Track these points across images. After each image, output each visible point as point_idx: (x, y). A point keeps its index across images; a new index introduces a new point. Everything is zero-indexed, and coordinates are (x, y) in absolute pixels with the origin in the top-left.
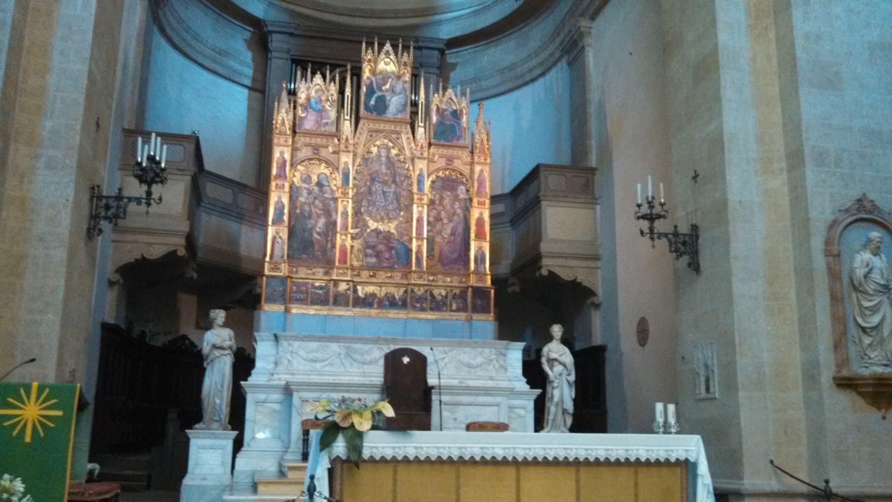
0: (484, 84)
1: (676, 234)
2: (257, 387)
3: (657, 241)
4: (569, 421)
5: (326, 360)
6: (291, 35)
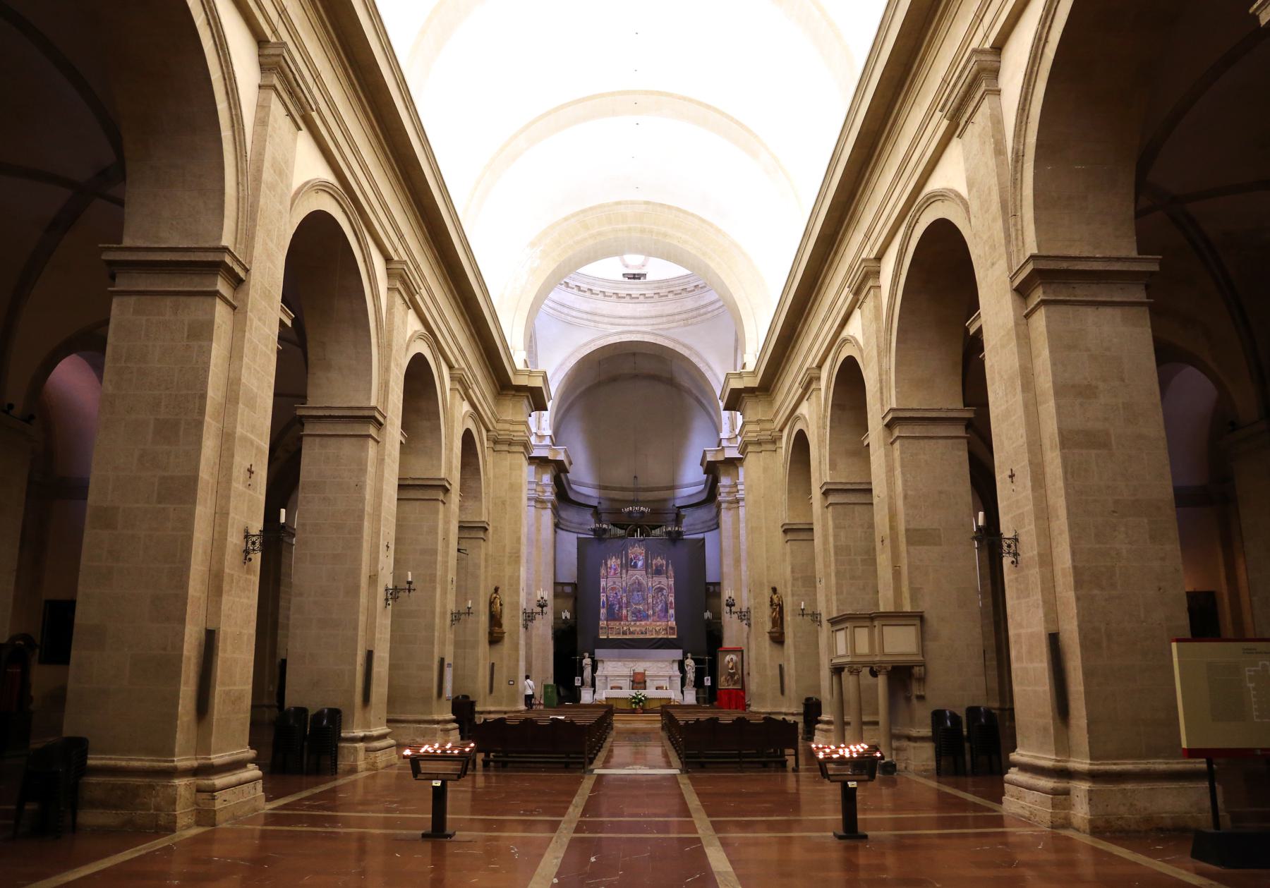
0: (697, 527)
1: (741, 612)
2: (598, 676)
3: (733, 615)
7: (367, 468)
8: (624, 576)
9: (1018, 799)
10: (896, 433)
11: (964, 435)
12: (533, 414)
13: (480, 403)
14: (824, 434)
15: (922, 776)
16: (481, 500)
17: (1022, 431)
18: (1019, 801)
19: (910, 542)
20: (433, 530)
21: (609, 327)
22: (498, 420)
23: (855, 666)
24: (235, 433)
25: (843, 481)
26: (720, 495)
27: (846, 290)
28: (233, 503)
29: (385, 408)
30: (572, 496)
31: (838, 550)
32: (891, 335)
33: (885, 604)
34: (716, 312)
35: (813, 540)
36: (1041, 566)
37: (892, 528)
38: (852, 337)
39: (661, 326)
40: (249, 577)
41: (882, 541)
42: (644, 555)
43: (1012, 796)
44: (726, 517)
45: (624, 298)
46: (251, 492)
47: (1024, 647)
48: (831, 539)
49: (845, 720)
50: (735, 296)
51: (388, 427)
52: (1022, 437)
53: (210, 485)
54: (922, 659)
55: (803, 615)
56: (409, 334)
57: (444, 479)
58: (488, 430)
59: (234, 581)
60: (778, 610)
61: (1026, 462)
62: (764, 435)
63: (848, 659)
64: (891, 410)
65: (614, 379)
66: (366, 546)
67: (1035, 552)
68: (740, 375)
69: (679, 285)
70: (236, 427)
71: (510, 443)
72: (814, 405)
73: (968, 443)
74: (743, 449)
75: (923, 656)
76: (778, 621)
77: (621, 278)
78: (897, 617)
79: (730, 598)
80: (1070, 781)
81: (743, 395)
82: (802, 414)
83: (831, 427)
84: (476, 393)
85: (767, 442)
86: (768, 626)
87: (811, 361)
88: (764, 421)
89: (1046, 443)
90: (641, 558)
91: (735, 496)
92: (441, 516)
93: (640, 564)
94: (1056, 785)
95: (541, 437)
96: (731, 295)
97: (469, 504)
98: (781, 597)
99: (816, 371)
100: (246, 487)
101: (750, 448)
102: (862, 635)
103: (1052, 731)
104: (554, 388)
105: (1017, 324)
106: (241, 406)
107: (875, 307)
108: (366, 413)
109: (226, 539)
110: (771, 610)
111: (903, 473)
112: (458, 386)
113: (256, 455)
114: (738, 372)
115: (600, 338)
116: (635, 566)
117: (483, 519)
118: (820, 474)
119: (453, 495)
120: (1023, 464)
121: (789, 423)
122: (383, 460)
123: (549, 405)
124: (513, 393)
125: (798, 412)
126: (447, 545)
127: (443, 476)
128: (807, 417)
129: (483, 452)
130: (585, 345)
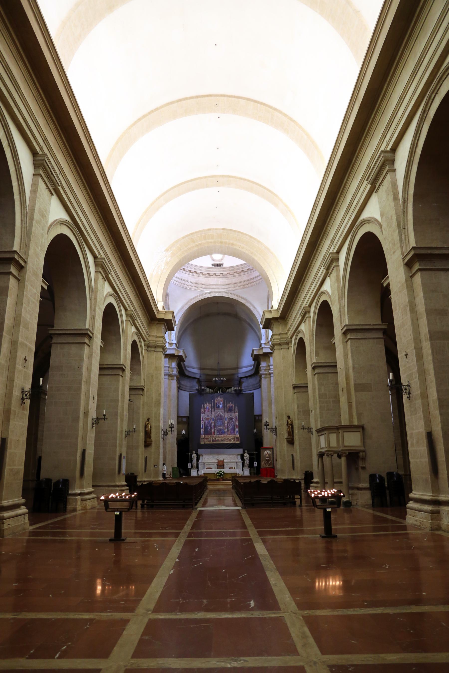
4: (248, 466)
6: (206, 381)
7: (84, 358)
8: (213, 412)
9: (414, 516)
10: (349, 337)
11: (382, 337)
12: (167, 332)
13: (141, 327)
14: (313, 339)
15: (364, 507)
16: (141, 375)
17: (411, 332)
18: (414, 518)
19: (356, 390)
20: (117, 390)
21: (205, 289)
22: (150, 336)
23: (330, 453)
24: (18, 341)
25: (323, 362)
26: (261, 371)
27: (322, 268)
28: (16, 376)
29: (93, 330)
30: (187, 373)
31: (320, 396)
32: (345, 289)
33: (345, 422)
34: (258, 282)
35: (308, 392)
36: (422, 399)
37: (348, 384)
38: (326, 291)
39: (231, 289)
40: (23, 412)
41: (343, 390)
43: (411, 515)
44: (264, 382)
45: (212, 275)
46: (25, 370)
47: (415, 440)
48: (317, 391)
49: (325, 481)
50: (267, 273)
51: (94, 339)
52: (411, 335)
53: (5, 367)
54: (364, 448)
55: (303, 429)
56: (105, 293)
57: (122, 365)
58: (144, 341)
59: (16, 414)
60: (291, 426)
61: (413, 347)
62: (283, 341)
63: (326, 450)
64: (346, 325)
65: (208, 315)
66: (83, 397)
67: (419, 392)
68: (270, 311)
69: (240, 269)
70: (18, 338)
71: (156, 347)
72: (308, 324)
73: (385, 341)
74: (272, 348)
75: (364, 447)
76: (291, 433)
77: (211, 266)
78: (350, 428)
79: (266, 421)
80: (440, 506)
81: (272, 321)
82: (301, 330)
83: (316, 335)
84: (139, 323)
85: (284, 344)
86: (286, 436)
87: (306, 303)
88: (282, 333)
89: (423, 337)
90: (221, 403)
91: (269, 371)
92: (121, 383)
93: (221, 406)
94: (433, 508)
95: (171, 344)
96: (266, 273)
97: (135, 377)
98: (292, 421)
99: (309, 308)
100: (23, 367)
101: (276, 347)
102: (333, 437)
103: (430, 481)
104: (178, 320)
105: (406, 281)
106: (21, 327)
107: (337, 276)
108: (84, 332)
109: (13, 393)
110: (287, 427)
111: (352, 356)
112: (130, 319)
113: (28, 352)
114: (269, 310)
115: (200, 295)
116: (219, 407)
117: (142, 385)
118: (311, 359)
119: (127, 373)
120: (411, 349)
121: (295, 334)
122: (92, 355)
123: (175, 328)
124: (157, 322)
125: (299, 329)
126: (124, 398)
127: (121, 363)
128: (304, 331)
129: (142, 351)
130: (193, 299)
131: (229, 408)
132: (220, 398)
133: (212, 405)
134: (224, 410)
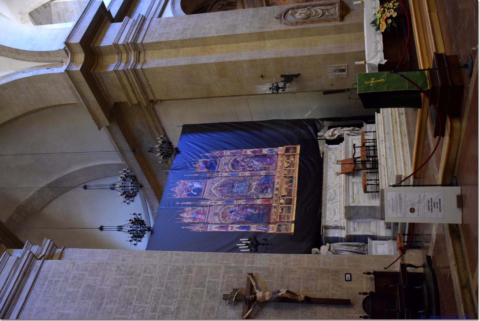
5: (334, 208)
8: (209, 203)
42: (186, 182)
90: (190, 184)
93: (197, 185)
116: (199, 190)
131: (207, 168)
132: (177, 188)
133: (188, 205)
134: (209, 178)
